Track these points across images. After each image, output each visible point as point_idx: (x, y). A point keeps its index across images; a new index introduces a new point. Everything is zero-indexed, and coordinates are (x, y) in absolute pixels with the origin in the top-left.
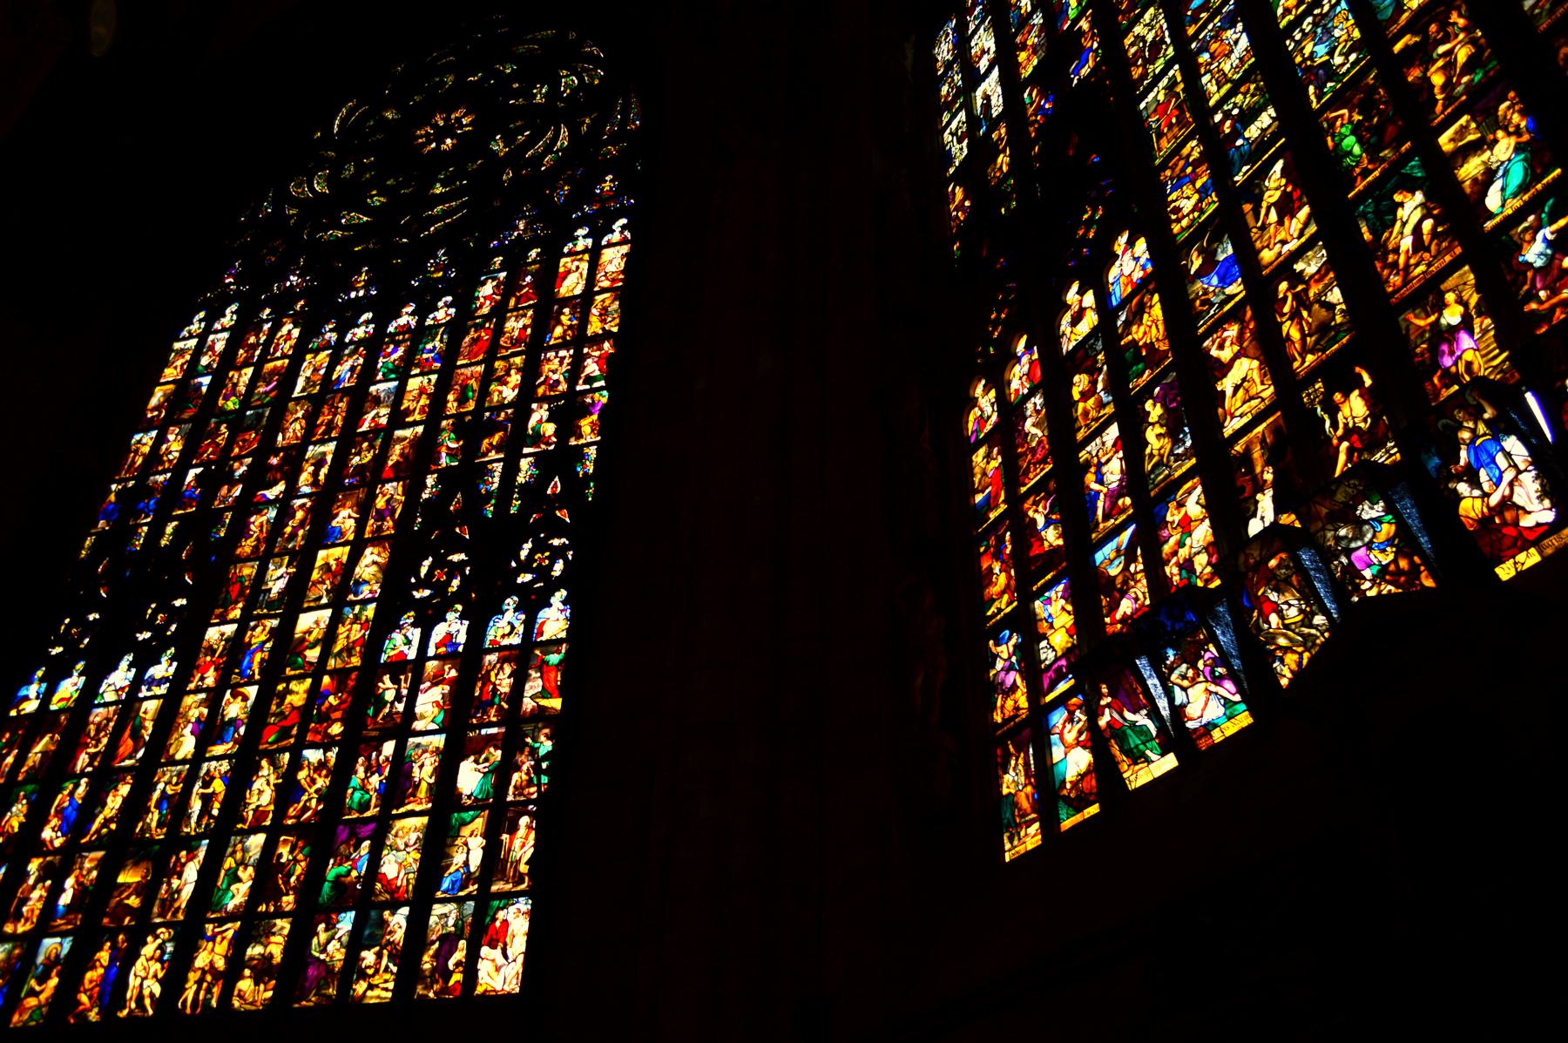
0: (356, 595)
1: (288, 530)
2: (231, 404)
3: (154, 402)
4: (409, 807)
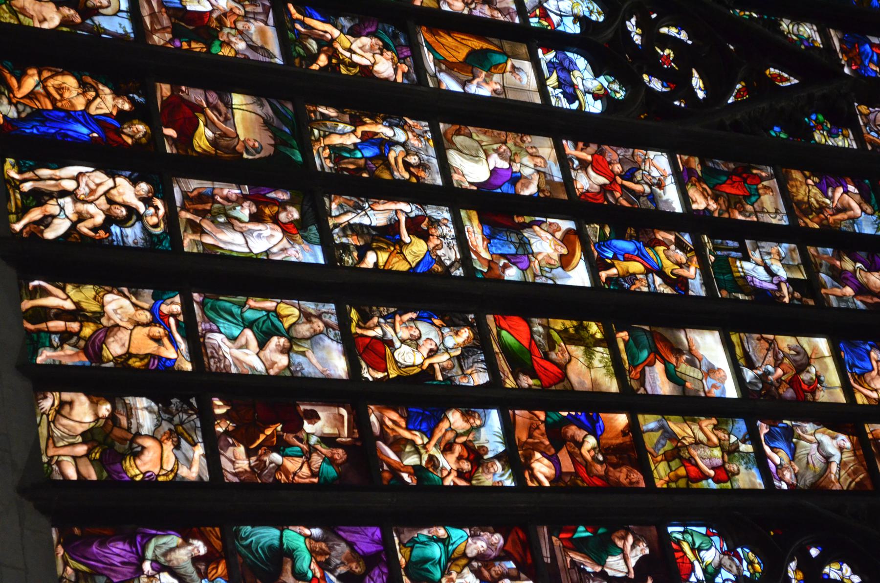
0: (770, 436)
1: (848, 265)
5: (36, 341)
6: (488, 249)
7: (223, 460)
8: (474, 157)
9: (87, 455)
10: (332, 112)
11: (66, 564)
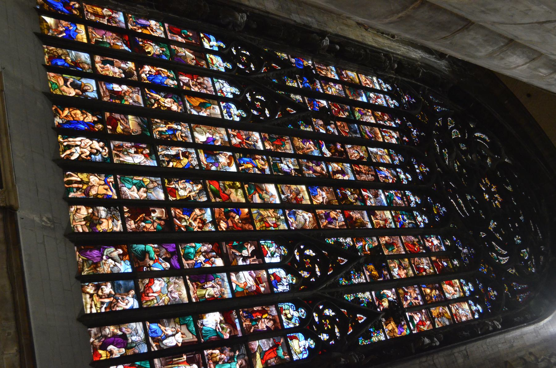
0: (289, 214)
1: (311, 164)
2: (357, 115)
3: (349, 73)
4: (191, 286)
5: (69, 190)
6: (206, 161)
7: (127, 225)
8: (202, 134)
9: (85, 225)
10: (159, 121)
11: (79, 257)
